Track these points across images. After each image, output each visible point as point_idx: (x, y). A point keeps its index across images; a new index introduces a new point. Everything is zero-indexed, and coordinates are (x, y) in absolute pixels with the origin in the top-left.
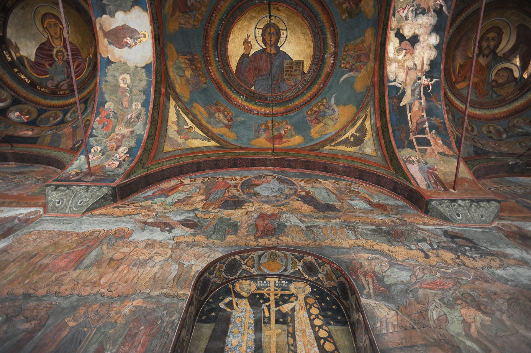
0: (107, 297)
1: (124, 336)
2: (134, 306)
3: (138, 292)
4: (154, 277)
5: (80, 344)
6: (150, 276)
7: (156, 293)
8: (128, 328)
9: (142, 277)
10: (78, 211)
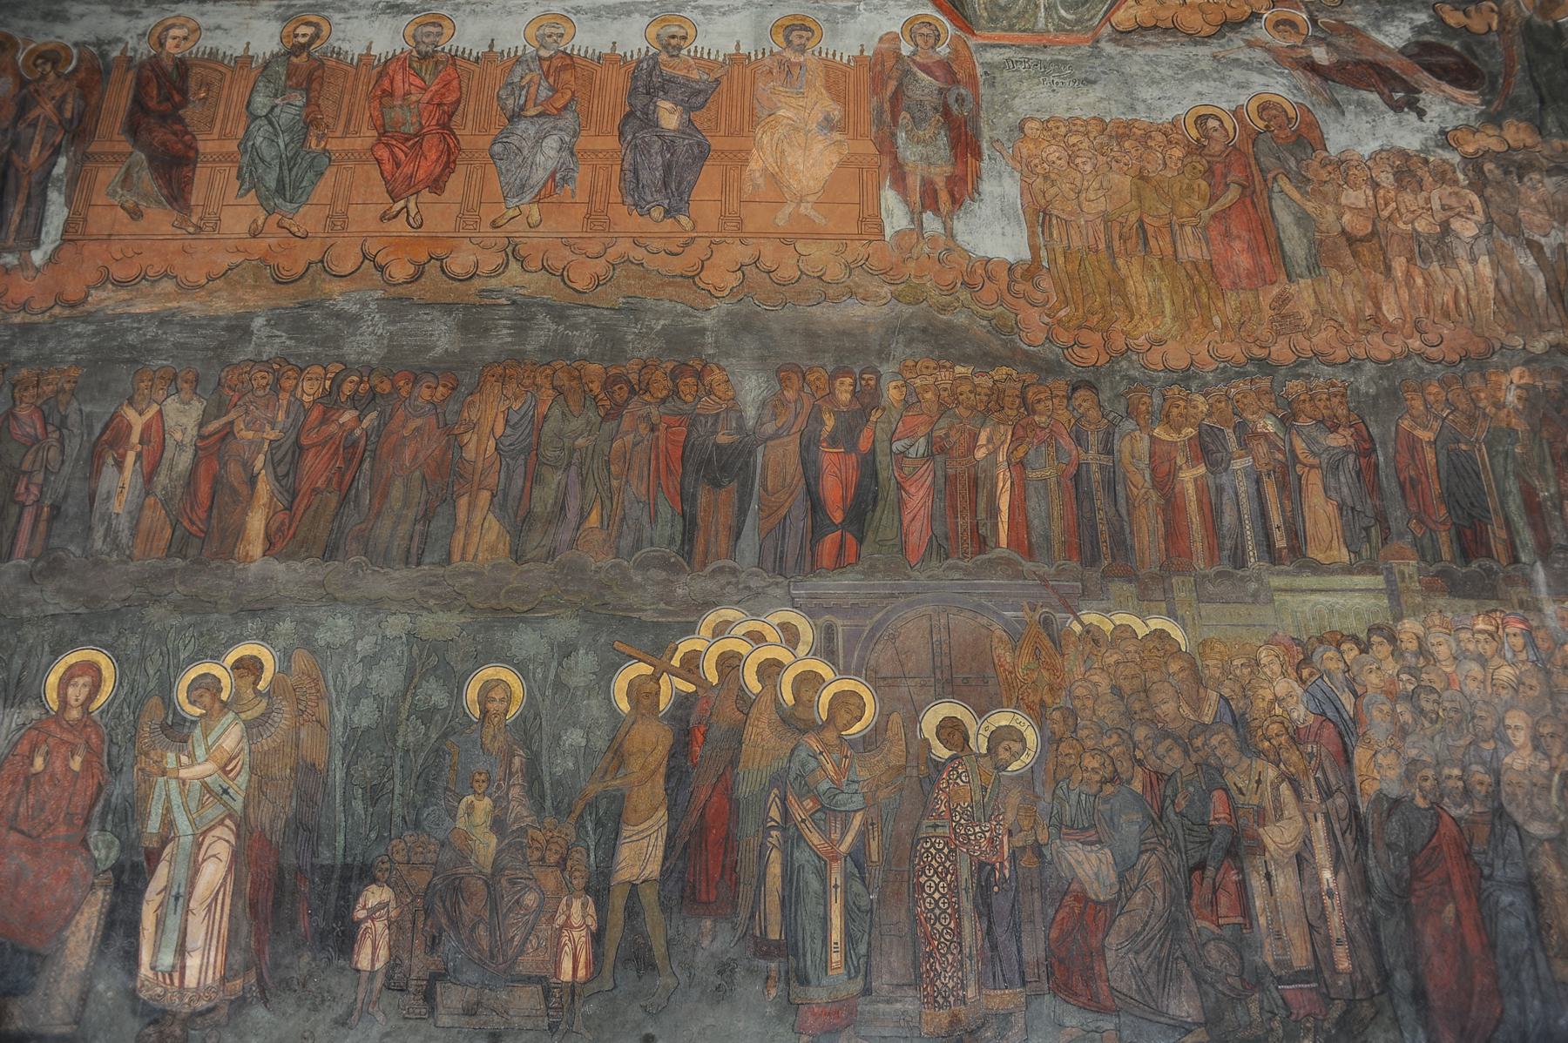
0: (1440, 363)
1: (1548, 458)
2: (1518, 387)
3: (1498, 346)
4: (1500, 296)
5: (1479, 478)
6: (1492, 295)
7: (1539, 346)
8: (1544, 441)
9: (1473, 295)
10: (1078, 22)
